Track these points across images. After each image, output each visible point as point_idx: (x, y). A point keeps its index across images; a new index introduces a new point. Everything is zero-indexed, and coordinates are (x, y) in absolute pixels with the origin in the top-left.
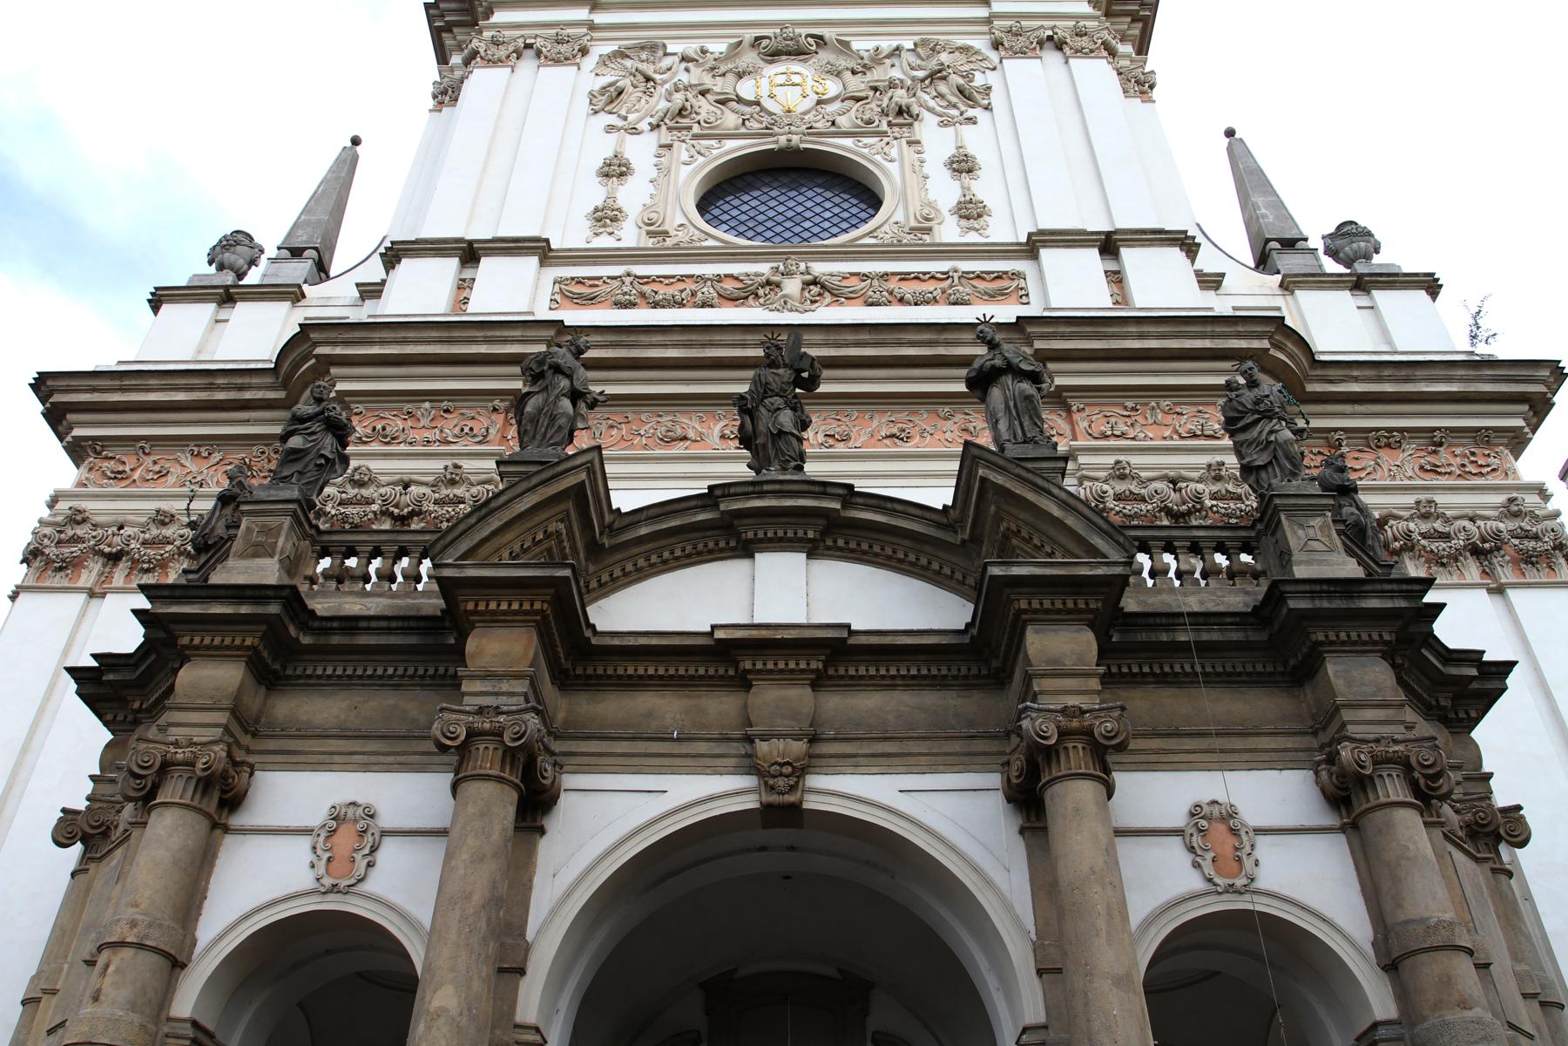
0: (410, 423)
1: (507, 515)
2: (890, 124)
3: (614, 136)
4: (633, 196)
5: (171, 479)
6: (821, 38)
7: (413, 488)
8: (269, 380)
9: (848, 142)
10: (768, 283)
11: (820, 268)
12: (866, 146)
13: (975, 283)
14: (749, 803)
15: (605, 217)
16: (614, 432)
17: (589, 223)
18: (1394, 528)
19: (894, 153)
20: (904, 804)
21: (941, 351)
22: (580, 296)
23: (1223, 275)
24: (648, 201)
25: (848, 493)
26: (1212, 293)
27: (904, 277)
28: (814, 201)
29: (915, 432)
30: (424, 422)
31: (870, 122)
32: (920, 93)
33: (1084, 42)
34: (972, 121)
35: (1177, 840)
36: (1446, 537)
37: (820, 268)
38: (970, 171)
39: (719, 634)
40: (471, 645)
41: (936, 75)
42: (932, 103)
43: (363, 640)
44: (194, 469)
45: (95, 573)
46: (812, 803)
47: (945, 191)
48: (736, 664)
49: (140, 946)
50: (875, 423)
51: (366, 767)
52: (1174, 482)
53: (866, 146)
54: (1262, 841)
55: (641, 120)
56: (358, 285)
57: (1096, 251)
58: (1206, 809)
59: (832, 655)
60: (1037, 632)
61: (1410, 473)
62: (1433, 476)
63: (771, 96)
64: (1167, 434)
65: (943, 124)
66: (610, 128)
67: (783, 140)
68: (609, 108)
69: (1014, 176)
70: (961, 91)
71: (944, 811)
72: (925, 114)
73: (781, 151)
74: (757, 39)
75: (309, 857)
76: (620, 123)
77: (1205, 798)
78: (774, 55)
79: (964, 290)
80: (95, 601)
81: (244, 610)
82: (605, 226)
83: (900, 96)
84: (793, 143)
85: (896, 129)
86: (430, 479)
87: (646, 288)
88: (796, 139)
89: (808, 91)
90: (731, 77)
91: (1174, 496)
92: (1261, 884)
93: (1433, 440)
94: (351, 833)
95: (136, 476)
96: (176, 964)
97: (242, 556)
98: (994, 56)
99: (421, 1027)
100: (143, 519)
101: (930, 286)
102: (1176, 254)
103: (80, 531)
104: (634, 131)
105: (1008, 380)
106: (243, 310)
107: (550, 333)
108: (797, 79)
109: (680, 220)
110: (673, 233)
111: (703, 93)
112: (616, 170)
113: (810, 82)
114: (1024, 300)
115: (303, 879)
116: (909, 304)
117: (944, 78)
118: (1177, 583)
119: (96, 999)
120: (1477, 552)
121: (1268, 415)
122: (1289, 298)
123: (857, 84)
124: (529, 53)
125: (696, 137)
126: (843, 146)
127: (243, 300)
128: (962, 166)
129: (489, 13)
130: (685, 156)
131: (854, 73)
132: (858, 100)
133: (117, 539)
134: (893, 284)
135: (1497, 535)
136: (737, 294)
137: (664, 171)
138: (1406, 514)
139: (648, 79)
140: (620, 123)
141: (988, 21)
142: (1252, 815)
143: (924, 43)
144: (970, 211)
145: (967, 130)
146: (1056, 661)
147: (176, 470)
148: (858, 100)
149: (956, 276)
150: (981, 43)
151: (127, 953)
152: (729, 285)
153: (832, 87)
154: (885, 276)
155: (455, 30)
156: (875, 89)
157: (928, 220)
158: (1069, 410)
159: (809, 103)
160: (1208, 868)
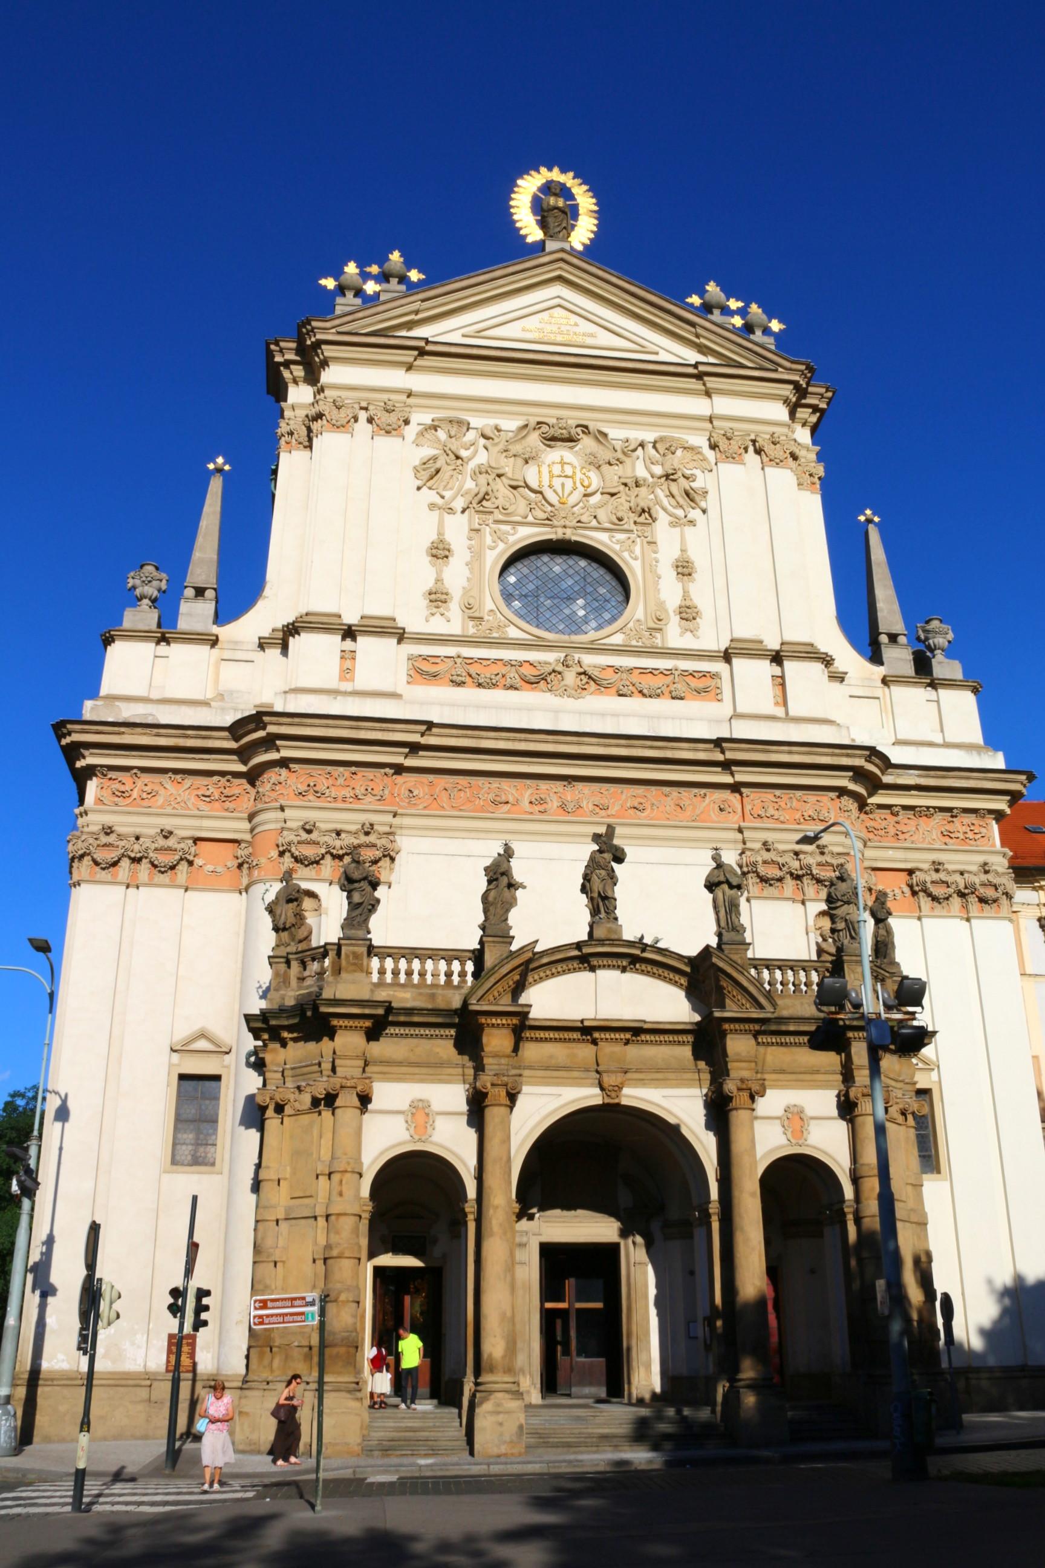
0: (331, 781)
1: (497, 976)
2: (635, 523)
3: (436, 513)
4: (456, 576)
5: (160, 800)
6: (586, 427)
7: (343, 835)
8: (226, 734)
9: (603, 537)
10: (554, 671)
11: (590, 660)
12: (618, 542)
13: (689, 679)
14: (598, 1101)
15: (437, 598)
16: (462, 794)
18: (919, 876)
19: (637, 550)
20: (664, 1103)
21: (669, 754)
22: (428, 674)
23: (846, 673)
24: (466, 584)
26: (836, 685)
27: (644, 671)
29: (648, 806)
30: (341, 781)
31: (620, 520)
32: (659, 491)
34: (692, 523)
35: (778, 1122)
37: (590, 660)
38: (690, 575)
39: (586, 1024)
40: (485, 1040)
42: (665, 502)
43: (416, 1019)
44: (175, 792)
45: (127, 870)
46: (625, 1101)
47: (670, 591)
48: (591, 1035)
49: (353, 1172)
50: (624, 797)
51: (422, 1081)
52: (796, 854)
53: (618, 542)
54: (812, 1122)
55: (454, 498)
56: (260, 638)
57: (768, 662)
58: (792, 1109)
59: (636, 1032)
60: (732, 1039)
61: (934, 837)
62: (947, 840)
63: (550, 487)
64: (797, 817)
65: (672, 525)
66: (432, 506)
67: (560, 531)
68: (429, 484)
69: (720, 582)
70: (687, 494)
71: (682, 1105)
72: (661, 515)
73: (559, 541)
74: (539, 423)
75: (405, 1125)
76: (440, 501)
77: (793, 1102)
78: (551, 440)
79: (680, 688)
80: (132, 891)
81: (367, 1011)
82: (437, 607)
83: (644, 498)
84: (567, 537)
85: (640, 528)
86: (353, 828)
88: (568, 532)
89: (578, 485)
90: (520, 461)
91: (796, 864)
92: (809, 1142)
94: (420, 1114)
95: (135, 794)
96: (361, 1175)
97: (347, 971)
98: (710, 455)
99: (491, 1212)
100: (153, 832)
101: (658, 682)
103: (111, 839)
105: (725, 887)
106: (177, 651)
107: (424, 728)
108: (569, 471)
110: (486, 618)
111: (499, 476)
112: (440, 552)
113: (579, 475)
114: (719, 697)
115: (406, 1136)
116: (644, 695)
117: (674, 480)
118: (792, 988)
119: (341, 1194)
120: (962, 895)
121: (848, 903)
122: (886, 689)
123: (613, 474)
124: (363, 416)
125: (497, 522)
126: (600, 540)
127: (175, 642)
128: (684, 569)
129: (325, 363)
130: (489, 540)
131: (610, 464)
132: (613, 495)
133: (137, 847)
134: (635, 678)
135: (973, 886)
136: (533, 679)
137: (477, 555)
138: (925, 866)
139: (458, 457)
140: (440, 501)
142: (810, 1112)
143: (662, 439)
144: (688, 614)
145: (688, 530)
146: (738, 1054)
147: (162, 791)
148: (613, 495)
149: (677, 673)
150: (700, 441)
151: (348, 1175)
152: (527, 671)
153: (595, 481)
154: (630, 670)
155: (292, 367)
156: (625, 485)
157: (660, 620)
158: (741, 794)
160: (789, 1134)
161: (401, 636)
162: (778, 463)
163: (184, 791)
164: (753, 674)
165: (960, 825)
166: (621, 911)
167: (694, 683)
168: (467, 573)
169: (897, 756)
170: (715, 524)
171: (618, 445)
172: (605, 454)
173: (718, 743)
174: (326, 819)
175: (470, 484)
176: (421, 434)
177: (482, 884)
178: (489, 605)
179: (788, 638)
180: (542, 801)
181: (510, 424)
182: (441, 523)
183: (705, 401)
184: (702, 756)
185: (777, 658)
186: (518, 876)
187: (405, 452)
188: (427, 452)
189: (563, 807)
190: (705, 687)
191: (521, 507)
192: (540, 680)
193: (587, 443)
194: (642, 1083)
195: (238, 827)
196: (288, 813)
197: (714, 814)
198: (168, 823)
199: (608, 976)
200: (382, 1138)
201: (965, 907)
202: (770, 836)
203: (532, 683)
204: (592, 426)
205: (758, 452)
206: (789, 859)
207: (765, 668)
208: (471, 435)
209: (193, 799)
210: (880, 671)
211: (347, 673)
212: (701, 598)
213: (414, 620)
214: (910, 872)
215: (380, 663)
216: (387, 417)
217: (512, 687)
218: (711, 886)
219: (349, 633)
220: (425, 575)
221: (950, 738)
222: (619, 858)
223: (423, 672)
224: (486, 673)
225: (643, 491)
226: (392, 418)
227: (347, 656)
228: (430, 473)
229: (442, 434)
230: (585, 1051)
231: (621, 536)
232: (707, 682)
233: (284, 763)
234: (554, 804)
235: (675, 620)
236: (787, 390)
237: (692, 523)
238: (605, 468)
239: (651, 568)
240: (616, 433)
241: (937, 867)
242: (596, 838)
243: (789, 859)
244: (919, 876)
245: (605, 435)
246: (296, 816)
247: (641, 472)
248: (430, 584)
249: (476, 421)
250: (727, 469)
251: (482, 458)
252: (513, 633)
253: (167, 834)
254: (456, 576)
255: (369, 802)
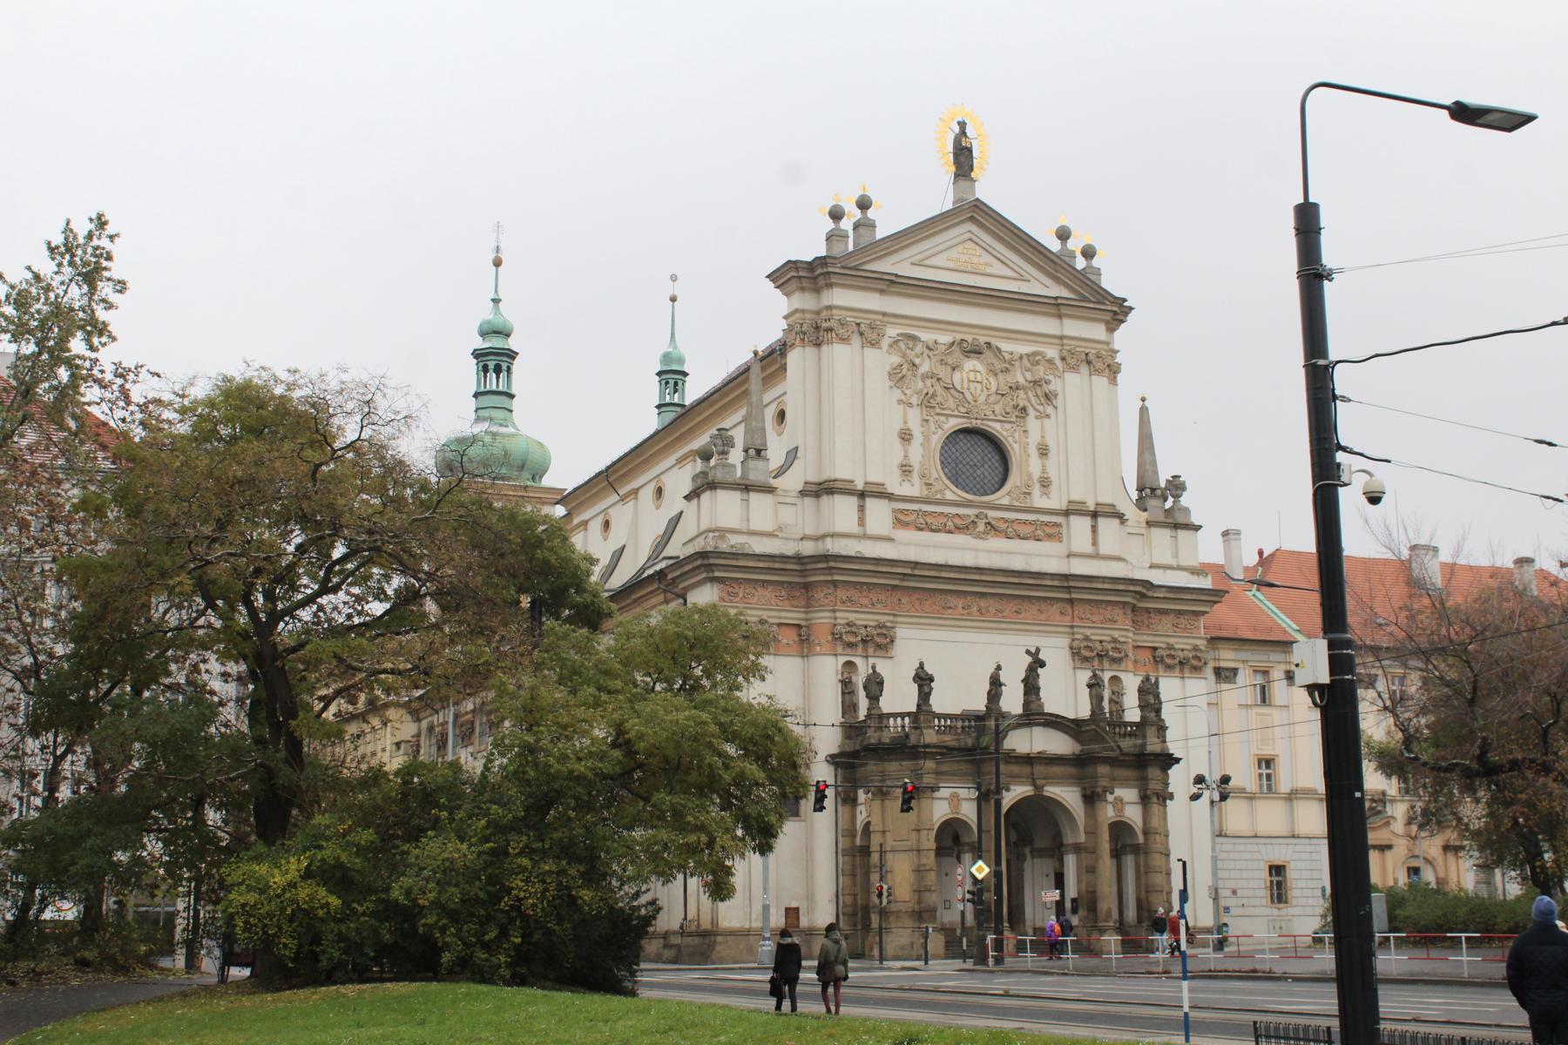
9: (997, 426)
15: (906, 470)
17: (899, 472)
25: (1057, 716)
28: (978, 452)
33: (1099, 365)
34: (1048, 416)
36: (1173, 657)
37: (992, 514)
41: (1036, 383)
47: (1035, 466)
66: (900, 402)
71: (1068, 795)
87: (929, 520)
93: (1179, 613)
94: (955, 800)
101: (1027, 530)
102: (1117, 521)
104: (910, 405)
109: (935, 475)
126: (997, 428)
128: (1043, 452)
137: (927, 438)
141: (1061, 338)
143: (1035, 354)
144: (1045, 483)
145: (1046, 421)
152: (958, 522)
159: (982, 399)
161: (890, 497)
162: (1098, 372)
163: (767, 594)
164: (1080, 525)
165: (1182, 621)
166: (1043, 694)
167: (1048, 530)
168: (920, 451)
169: (1158, 578)
170: (1061, 417)
171: (1007, 356)
172: (998, 366)
173: (1066, 577)
174: (861, 619)
175: (920, 385)
176: (891, 346)
177: (987, 687)
178: (935, 475)
179: (1101, 500)
180: (969, 607)
181: (945, 339)
182: (905, 416)
183: (1056, 322)
184: (1056, 583)
185: (1095, 515)
186: (1002, 680)
187: (880, 361)
188: (895, 359)
189: (979, 611)
190: (1052, 533)
191: (951, 403)
192: (963, 528)
193: (988, 353)
194: (1053, 784)
195: (794, 616)
196: (838, 614)
197: (1058, 617)
198: (764, 614)
199: (1037, 730)
200: (939, 809)
201: (1182, 671)
202: (1088, 632)
203: (959, 529)
204: (994, 341)
205: (1089, 363)
206: (1098, 646)
207: (1087, 521)
208: (919, 348)
209: (774, 600)
210: (1145, 514)
211: (862, 522)
212: (1052, 473)
213: (895, 486)
214: (1155, 649)
215: (879, 515)
216: (868, 332)
217: (950, 532)
218: (1090, 686)
219: (862, 495)
220: (897, 452)
221: (1184, 562)
222: (1042, 664)
223: (900, 522)
224: (935, 522)
225: (1021, 392)
226: (872, 336)
227: (862, 509)
228: (898, 377)
229: (902, 345)
230: (1026, 769)
231: (1007, 426)
232: (1055, 530)
233: (835, 584)
234: (975, 609)
235: (1037, 486)
236: (1108, 317)
237: (1048, 416)
238: (1000, 376)
239: (1025, 447)
240: (1006, 346)
241: (1170, 647)
242: (1028, 652)
243: (1098, 646)
244: (1160, 652)
245: (999, 350)
246: (843, 617)
247: (1021, 380)
248: (899, 459)
249: (926, 336)
250: (1069, 376)
251: (925, 367)
252: (949, 496)
253: (763, 622)
254: (916, 453)
255: (879, 608)
